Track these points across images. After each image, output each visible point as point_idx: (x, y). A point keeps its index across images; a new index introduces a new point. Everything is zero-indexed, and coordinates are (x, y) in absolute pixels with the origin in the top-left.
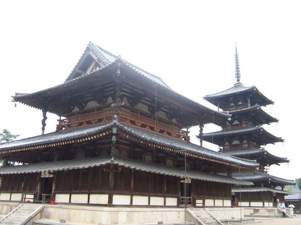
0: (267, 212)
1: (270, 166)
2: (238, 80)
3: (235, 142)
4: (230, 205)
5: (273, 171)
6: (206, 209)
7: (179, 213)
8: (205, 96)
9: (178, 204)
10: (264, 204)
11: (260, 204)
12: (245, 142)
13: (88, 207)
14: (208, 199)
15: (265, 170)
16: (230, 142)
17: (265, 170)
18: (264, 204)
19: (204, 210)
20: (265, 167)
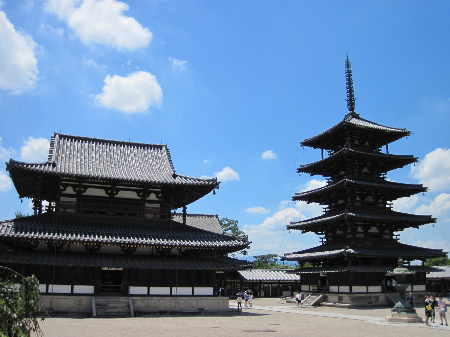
0: (350, 301)
1: (402, 230)
2: (352, 109)
3: (340, 202)
4: (212, 293)
5: (406, 237)
6: (129, 298)
7: (80, 301)
8: (303, 141)
9: (95, 292)
10: (351, 289)
11: (345, 289)
12: (349, 200)
13: (72, 297)
14: (303, 285)
15: (394, 237)
16: (363, 197)
17: (394, 237)
18: (351, 289)
19: (128, 299)
20: (395, 233)
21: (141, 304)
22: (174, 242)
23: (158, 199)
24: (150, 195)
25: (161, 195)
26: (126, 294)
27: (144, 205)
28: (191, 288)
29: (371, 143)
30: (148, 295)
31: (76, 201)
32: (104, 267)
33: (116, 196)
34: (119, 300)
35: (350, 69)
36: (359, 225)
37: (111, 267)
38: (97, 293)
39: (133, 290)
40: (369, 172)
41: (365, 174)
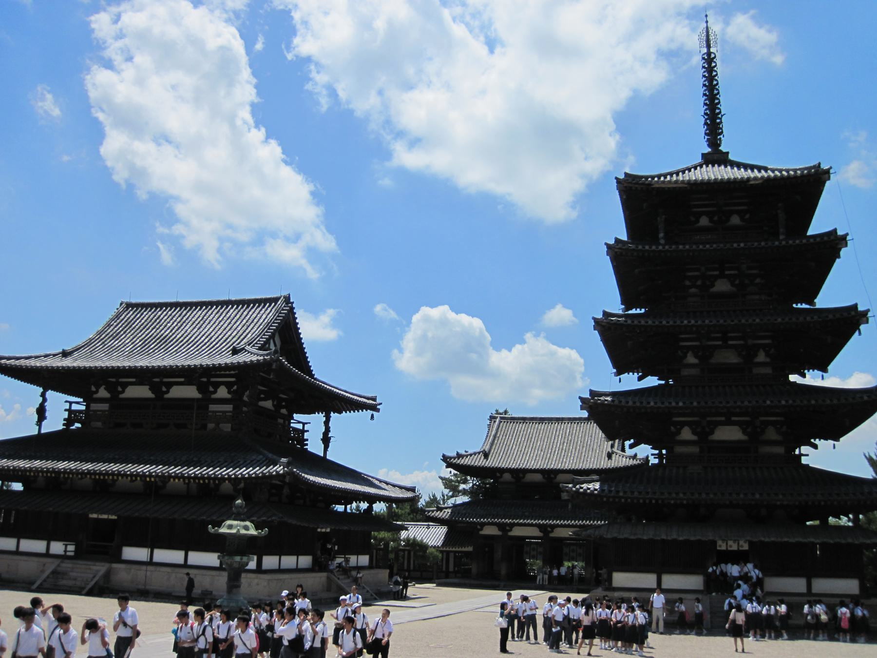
21: (123, 575)
22: (174, 470)
23: (229, 396)
24: (219, 390)
25: (235, 387)
26: (117, 557)
27: (208, 408)
28: (277, 558)
29: (716, 218)
30: (151, 563)
31: (107, 409)
32: (92, 513)
33: (166, 396)
34: (92, 567)
35: (712, 50)
36: (683, 424)
37: (102, 513)
38: (79, 555)
39: (132, 553)
40: (734, 289)
41: (721, 295)
